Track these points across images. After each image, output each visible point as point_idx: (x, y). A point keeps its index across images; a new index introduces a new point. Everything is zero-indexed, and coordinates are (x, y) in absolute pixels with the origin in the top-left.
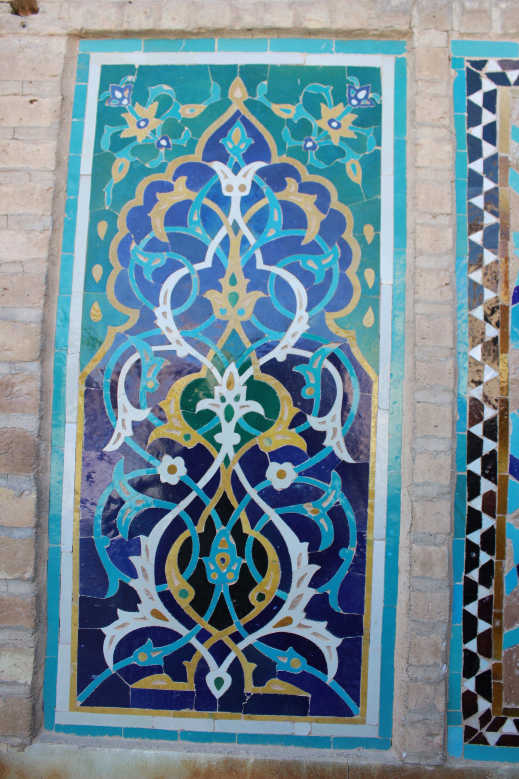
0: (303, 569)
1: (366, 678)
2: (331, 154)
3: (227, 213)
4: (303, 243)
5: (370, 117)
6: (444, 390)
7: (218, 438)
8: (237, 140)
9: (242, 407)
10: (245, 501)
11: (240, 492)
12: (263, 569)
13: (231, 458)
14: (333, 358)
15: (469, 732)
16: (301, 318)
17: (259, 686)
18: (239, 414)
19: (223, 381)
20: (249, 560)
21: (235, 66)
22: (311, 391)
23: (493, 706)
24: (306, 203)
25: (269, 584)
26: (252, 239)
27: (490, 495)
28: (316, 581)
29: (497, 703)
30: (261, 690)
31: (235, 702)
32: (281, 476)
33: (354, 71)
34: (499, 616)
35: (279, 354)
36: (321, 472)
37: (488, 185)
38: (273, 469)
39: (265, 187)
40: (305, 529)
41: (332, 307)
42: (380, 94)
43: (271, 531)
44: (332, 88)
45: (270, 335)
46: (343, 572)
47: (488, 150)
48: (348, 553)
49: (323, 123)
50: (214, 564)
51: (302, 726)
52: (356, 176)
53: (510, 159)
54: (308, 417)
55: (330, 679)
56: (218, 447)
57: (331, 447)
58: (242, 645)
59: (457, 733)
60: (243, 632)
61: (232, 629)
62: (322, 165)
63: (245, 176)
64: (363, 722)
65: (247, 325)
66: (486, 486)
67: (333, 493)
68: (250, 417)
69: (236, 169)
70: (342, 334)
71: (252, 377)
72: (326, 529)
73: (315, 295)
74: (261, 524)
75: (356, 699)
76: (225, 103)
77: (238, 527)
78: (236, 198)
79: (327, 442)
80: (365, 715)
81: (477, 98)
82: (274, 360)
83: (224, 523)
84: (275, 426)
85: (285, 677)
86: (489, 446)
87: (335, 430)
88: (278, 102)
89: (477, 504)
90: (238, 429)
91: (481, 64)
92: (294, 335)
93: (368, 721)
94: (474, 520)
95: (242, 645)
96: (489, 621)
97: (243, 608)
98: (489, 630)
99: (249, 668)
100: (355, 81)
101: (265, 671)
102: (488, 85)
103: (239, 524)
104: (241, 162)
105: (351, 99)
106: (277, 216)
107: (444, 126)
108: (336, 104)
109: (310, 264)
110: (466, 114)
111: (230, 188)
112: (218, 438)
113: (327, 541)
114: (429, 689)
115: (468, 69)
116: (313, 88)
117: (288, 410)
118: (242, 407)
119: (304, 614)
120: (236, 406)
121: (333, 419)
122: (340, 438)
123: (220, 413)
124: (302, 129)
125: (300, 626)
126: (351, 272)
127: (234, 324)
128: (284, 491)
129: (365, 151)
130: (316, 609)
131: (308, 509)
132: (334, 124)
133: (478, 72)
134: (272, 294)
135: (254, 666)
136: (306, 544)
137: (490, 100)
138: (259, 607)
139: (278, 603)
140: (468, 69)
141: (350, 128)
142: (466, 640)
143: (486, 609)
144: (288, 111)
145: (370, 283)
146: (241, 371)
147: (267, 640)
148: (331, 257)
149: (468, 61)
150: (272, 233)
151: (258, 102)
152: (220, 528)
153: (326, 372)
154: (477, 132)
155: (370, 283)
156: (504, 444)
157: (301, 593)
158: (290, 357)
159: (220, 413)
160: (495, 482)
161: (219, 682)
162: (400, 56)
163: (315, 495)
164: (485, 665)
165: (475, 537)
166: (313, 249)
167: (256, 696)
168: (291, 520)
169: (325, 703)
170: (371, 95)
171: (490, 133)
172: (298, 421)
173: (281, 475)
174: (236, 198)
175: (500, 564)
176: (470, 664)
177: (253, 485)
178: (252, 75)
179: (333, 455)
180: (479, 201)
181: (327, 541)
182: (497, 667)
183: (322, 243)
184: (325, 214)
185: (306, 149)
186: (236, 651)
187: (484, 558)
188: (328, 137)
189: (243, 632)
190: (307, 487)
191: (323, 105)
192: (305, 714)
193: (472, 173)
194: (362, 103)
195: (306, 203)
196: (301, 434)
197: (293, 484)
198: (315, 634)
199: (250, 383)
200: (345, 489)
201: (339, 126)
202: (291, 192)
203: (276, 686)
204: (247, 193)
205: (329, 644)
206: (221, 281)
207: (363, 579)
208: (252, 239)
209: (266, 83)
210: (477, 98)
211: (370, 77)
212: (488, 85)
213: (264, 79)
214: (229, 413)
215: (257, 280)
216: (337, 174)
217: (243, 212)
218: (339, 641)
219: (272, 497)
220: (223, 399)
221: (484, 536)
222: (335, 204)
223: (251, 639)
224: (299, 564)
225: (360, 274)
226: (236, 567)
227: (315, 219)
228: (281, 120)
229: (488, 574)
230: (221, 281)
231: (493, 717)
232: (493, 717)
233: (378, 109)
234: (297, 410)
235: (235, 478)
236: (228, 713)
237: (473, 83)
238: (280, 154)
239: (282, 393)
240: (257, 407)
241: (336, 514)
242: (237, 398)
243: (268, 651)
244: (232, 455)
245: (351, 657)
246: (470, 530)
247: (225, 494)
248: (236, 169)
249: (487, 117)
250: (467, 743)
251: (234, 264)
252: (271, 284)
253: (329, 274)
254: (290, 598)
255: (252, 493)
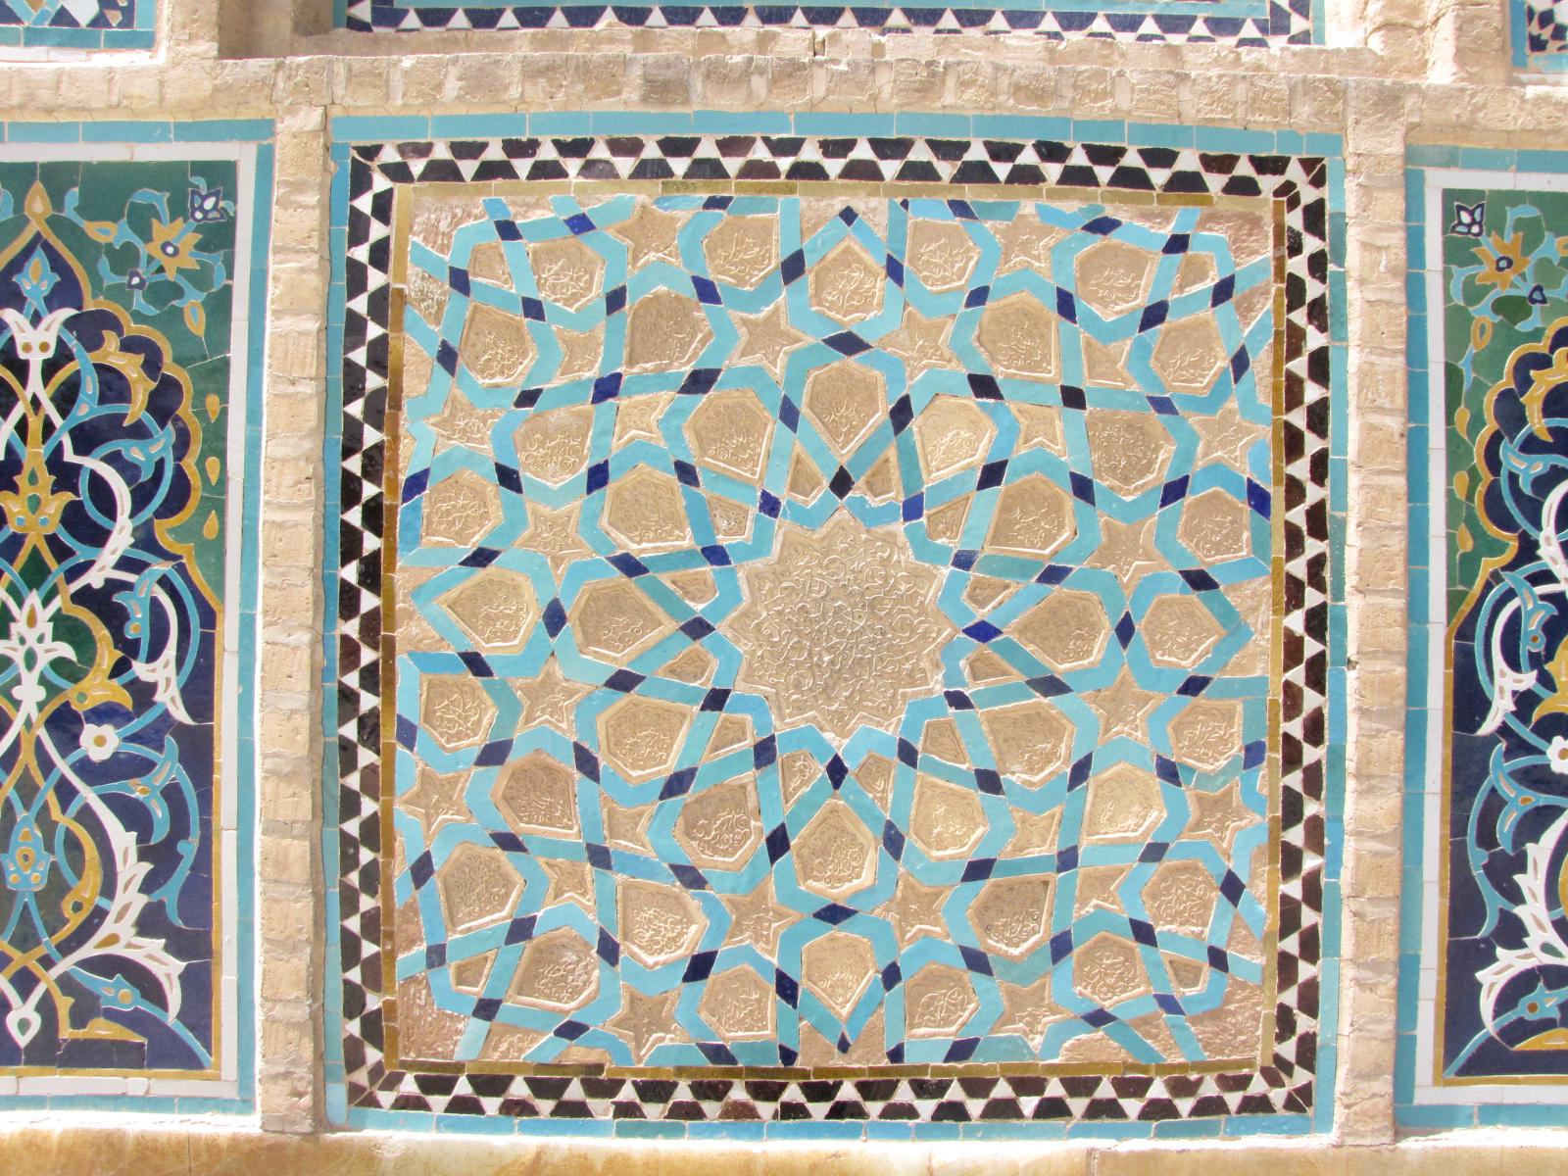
0: (132, 870)
1: (219, 1016)
2: (164, 293)
3: (24, 382)
4: (126, 424)
5: (219, 236)
6: (301, 626)
7: (17, 692)
8: (36, 281)
9: (48, 651)
10: (54, 778)
11: (47, 766)
12: (79, 871)
13: (34, 720)
14: (165, 582)
15: (355, 1091)
16: (122, 529)
17: (79, 1028)
18: (43, 661)
19: (20, 615)
20: (60, 856)
21: (34, 164)
22: (138, 627)
23: (386, 1057)
24: (130, 366)
25: (87, 888)
26: (57, 420)
27: (371, 769)
28: (149, 885)
29: (392, 1052)
30: (81, 1034)
31: (47, 1052)
32: (100, 742)
33: (200, 168)
34: (390, 935)
35: (95, 579)
36: (152, 737)
37: (374, 331)
38: (89, 732)
39: (73, 343)
40: (134, 815)
41: (160, 514)
42: (235, 202)
43: (87, 816)
44: (168, 194)
45: (82, 552)
46: (183, 872)
47: (375, 279)
48: (188, 848)
49: (153, 248)
50: (14, 862)
51: (136, 1082)
52: (196, 322)
53: (407, 291)
54: (134, 663)
55: (171, 1018)
56: (17, 704)
57: (163, 704)
58: (55, 972)
59: (337, 1093)
60: (55, 954)
61: (40, 951)
62: (152, 311)
63: (47, 329)
64: (218, 1078)
65: (52, 540)
66: (366, 757)
67: (169, 767)
68: (59, 665)
69: (36, 319)
70: (176, 549)
71: (59, 610)
72: (160, 815)
73: (142, 497)
74: (75, 807)
75: (208, 1046)
76: (20, 222)
77: (44, 813)
78: (36, 361)
79: (159, 697)
80: (219, 1067)
81: (364, 203)
82: (88, 587)
83: (27, 806)
84: (90, 676)
85: (113, 1015)
86: (368, 701)
87: (168, 680)
88: (91, 218)
89: (354, 781)
90: (43, 681)
91: (371, 152)
92: (113, 552)
93: (224, 1075)
94: (349, 804)
95: (55, 972)
96: (376, 941)
97: (54, 924)
98: (377, 955)
99: (64, 1004)
100: (200, 182)
101: (86, 1008)
102: (380, 183)
103: (45, 808)
104: (42, 307)
105: (194, 209)
106: (90, 386)
107: (312, 250)
108: (173, 219)
109: (134, 452)
110: (347, 228)
111: (27, 348)
112: (17, 692)
113: (160, 834)
114: (293, 1035)
115: (354, 160)
116: (143, 196)
117: (107, 655)
118: (48, 651)
119: (133, 931)
120: (39, 649)
121: (166, 666)
122: (175, 691)
123: (19, 657)
124: (124, 258)
125: (130, 945)
126: (189, 464)
127: (35, 540)
128: (103, 763)
129: (212, 286)
130: (150, 923)
131: (136, 789)
132: (170, 250)
133: (369, 163)
134: (84, 495)
135: (71, 1000)
136: (134, 835)
137: (382, 207)
138: (75, 921)
139: (100, 914)
140: (354, 160)
141: (192, 255)
142: (346, 967)
143: (372, 925)
144: (106, 233)
145: (214, 478)
146: (46, 602)
147: (88, 964)
148: (162, 441)
149: (355, 148)
150: (86, 408)
151: (65, 219)
152: (21, 813)
153: (155, 604)
154: (361, 253)
155: (214, 478)
156: (389, 701)
157: (131, 899)
158: (108, 581)
159: (19, 657)
160: (378, 752)
161: (24, 1025)
162: (265, 143)
163: (145, 767)
164: (373, 1002)
165: (353, 827)
166: (139, 432)
167: (75, 1041)
168: (114, 802)
169: (166, 1051)
170: (222, 204)
171: (380, 255)
172: (120, 668)
173: (100, 741)
174: (36, 361)
175: (387, 865)
176: (353, 1002)
177: (64, 755)
178: (57, 177)
179: (166, 714)
180: (360, 356)
181: (160, 834)
182: (390, 1007)
183: (150, 421)
184: (154, 380)
185: (130, 286)
186: (48, 980)
187: (366, 855)
188: (161, 270)
189: (55, 954)
190: (133, 758)
191: (154, 221)
192: (141, 1067)
193: (351, 315)
194: (210, 216)
195: (130, 366)
196: (126, 686)
197: (116, 754)
198: (150, 957)
199: (58, 619)
200: (183, 759)
201: (177, 251)
202: (111, 353)
203: (101, 1029)
204: (50, 354)
205: (168, 969)
206: (16, 478)
207: (209, 881)
208: (57, 420)
209: (76, 190)
210: (364, 203)
211: (222, 176)
212: (380, 183)
213: (75, 185)
214: (31, 659)
215: (64, 475)
216: (172, 320)
217: (46, 383)
218: (180, 965)
219: (88, 770)
220: (22, 641)
221: (363, 825)
222: (170, 368)
223: (66, 965)
224: (125, 861)
225: (201, 464)
226: (43, 867)
227: (142, 388)
228: (96, 245)
229: (372, 879)
230: (16, 478)
231: (387, 1072)
232: (387, 1072)
233: (231, 223)
234: (119, 654)
235: (39, 743)
236: (37, 1068)
237: (360, 181)
238: (95, 296)
239: (101, 632)
240: (66, 651)
241: (172, 794)
242: (41, 639)
243: (87, 978)
244: (35, 715)
245: (199, 986)
246: (344, 818)
247: (27, 769)
248: (36, 319)
249: (377, 230)
250: (352, 1107)
251: (34, 455)
252: (83, 484)
253: (160, 465)
254: (114, 908)
255: (63, 767)
